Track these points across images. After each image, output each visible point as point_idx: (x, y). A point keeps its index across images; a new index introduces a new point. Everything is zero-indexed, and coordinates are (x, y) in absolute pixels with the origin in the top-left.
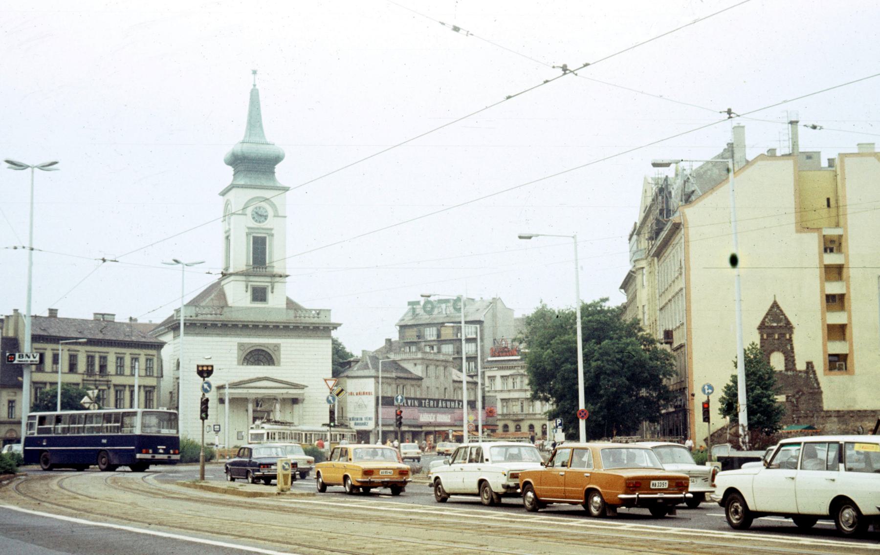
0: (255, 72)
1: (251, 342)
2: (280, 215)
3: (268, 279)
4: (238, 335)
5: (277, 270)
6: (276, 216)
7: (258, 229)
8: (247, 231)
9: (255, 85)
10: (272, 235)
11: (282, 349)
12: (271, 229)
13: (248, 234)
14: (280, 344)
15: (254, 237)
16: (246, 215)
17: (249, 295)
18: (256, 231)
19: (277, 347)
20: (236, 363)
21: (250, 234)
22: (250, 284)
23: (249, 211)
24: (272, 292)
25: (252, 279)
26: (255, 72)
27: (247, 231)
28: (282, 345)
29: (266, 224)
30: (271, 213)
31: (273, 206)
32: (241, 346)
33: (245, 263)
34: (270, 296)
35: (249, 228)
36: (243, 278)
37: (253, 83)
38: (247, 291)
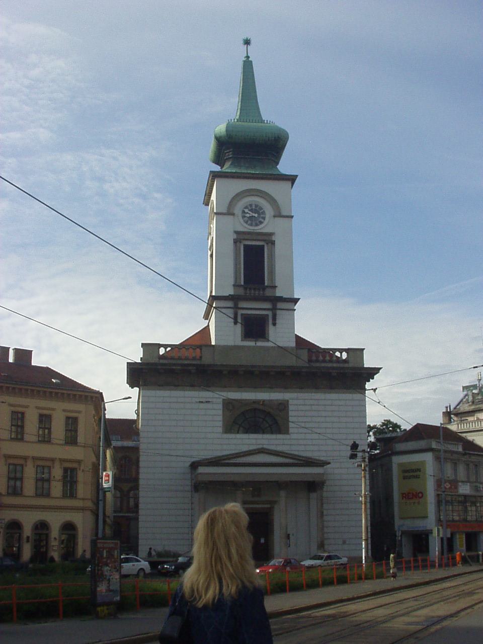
0: (247, 42)
1: (244, 398)
2: (284, 213)
3: (268, 305)
4: (225, 387)
5: (279, 293)
6: (278, 215)
7: (249, 233)
8: (235, 236)
9: (248, 57)
10: (273, 243)
11: (291, 408)
12: (271, 234)
13: (235, 241)
14: (288, 401)
15: (246, 247)
16: (233, 214)
17: (239, 329)
18: (247, 237)
19: (283, 406)
20: (220, 430)
21: (240, 242)
22: (240, 312)
23: (238, 209)
24: (274, 324)
25: (242, 304)
26: (247, 42)
27: (235, 236)
28: (291, 402)
29: (266, 227)
30: (269, 211)
31: (273, 201)
32: (228, 405)
33: (231, 281)
34: (271, 330)
35: (236, 232)
36: (230, 304)
37: (246, 55)
38: (236, 323)
